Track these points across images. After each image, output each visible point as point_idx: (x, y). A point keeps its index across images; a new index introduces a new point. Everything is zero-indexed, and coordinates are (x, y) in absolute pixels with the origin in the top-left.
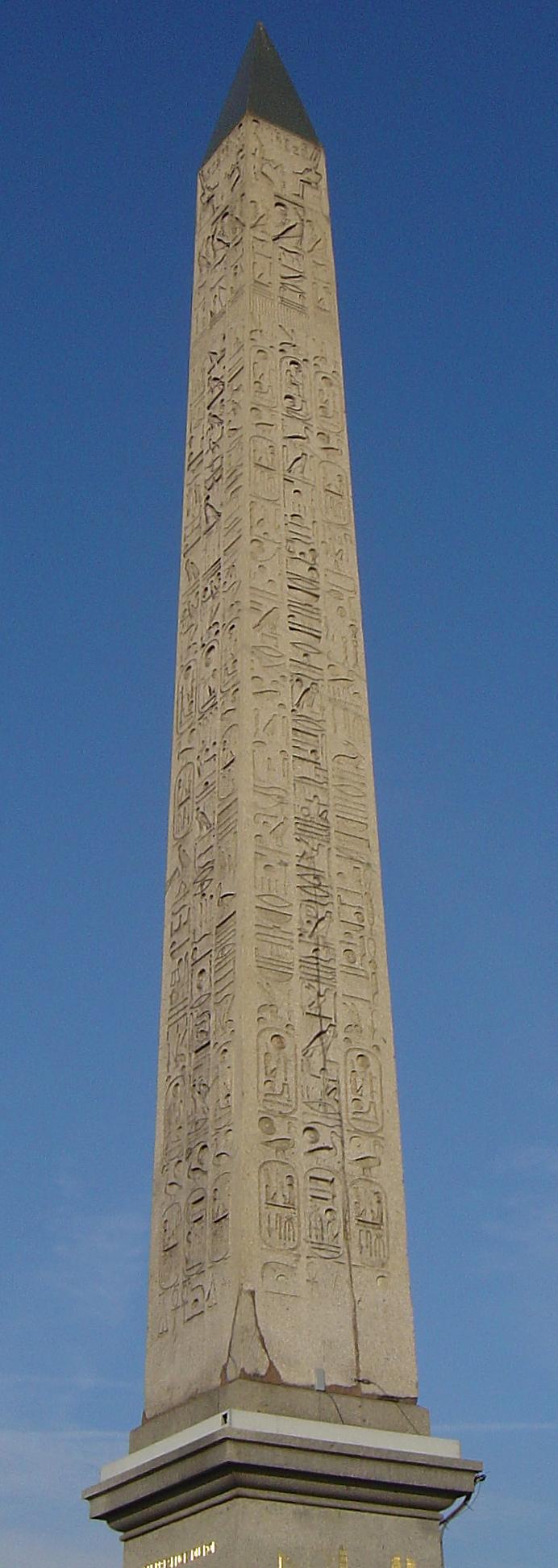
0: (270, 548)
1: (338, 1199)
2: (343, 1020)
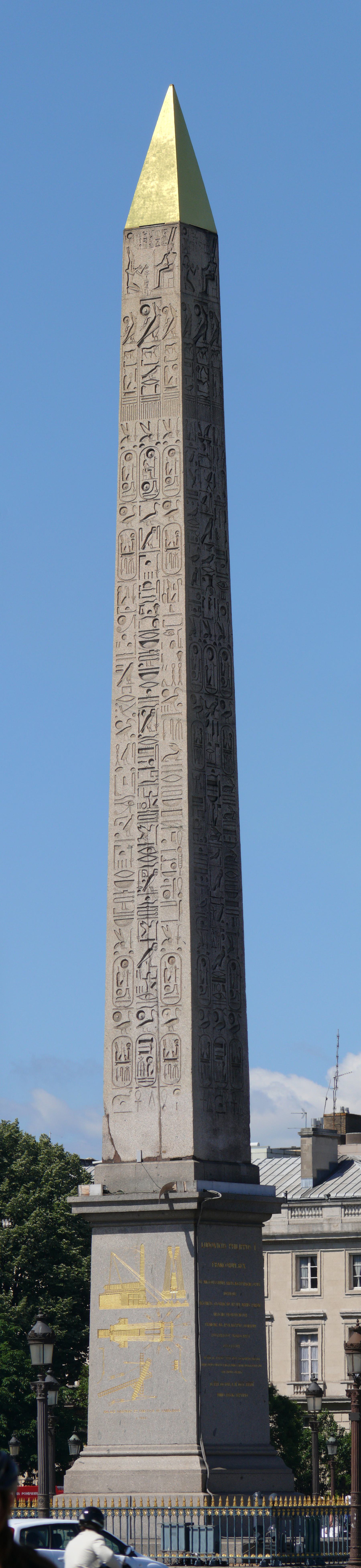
0: (129, 616)
1: (154, 1050)
2: (161, 937)
